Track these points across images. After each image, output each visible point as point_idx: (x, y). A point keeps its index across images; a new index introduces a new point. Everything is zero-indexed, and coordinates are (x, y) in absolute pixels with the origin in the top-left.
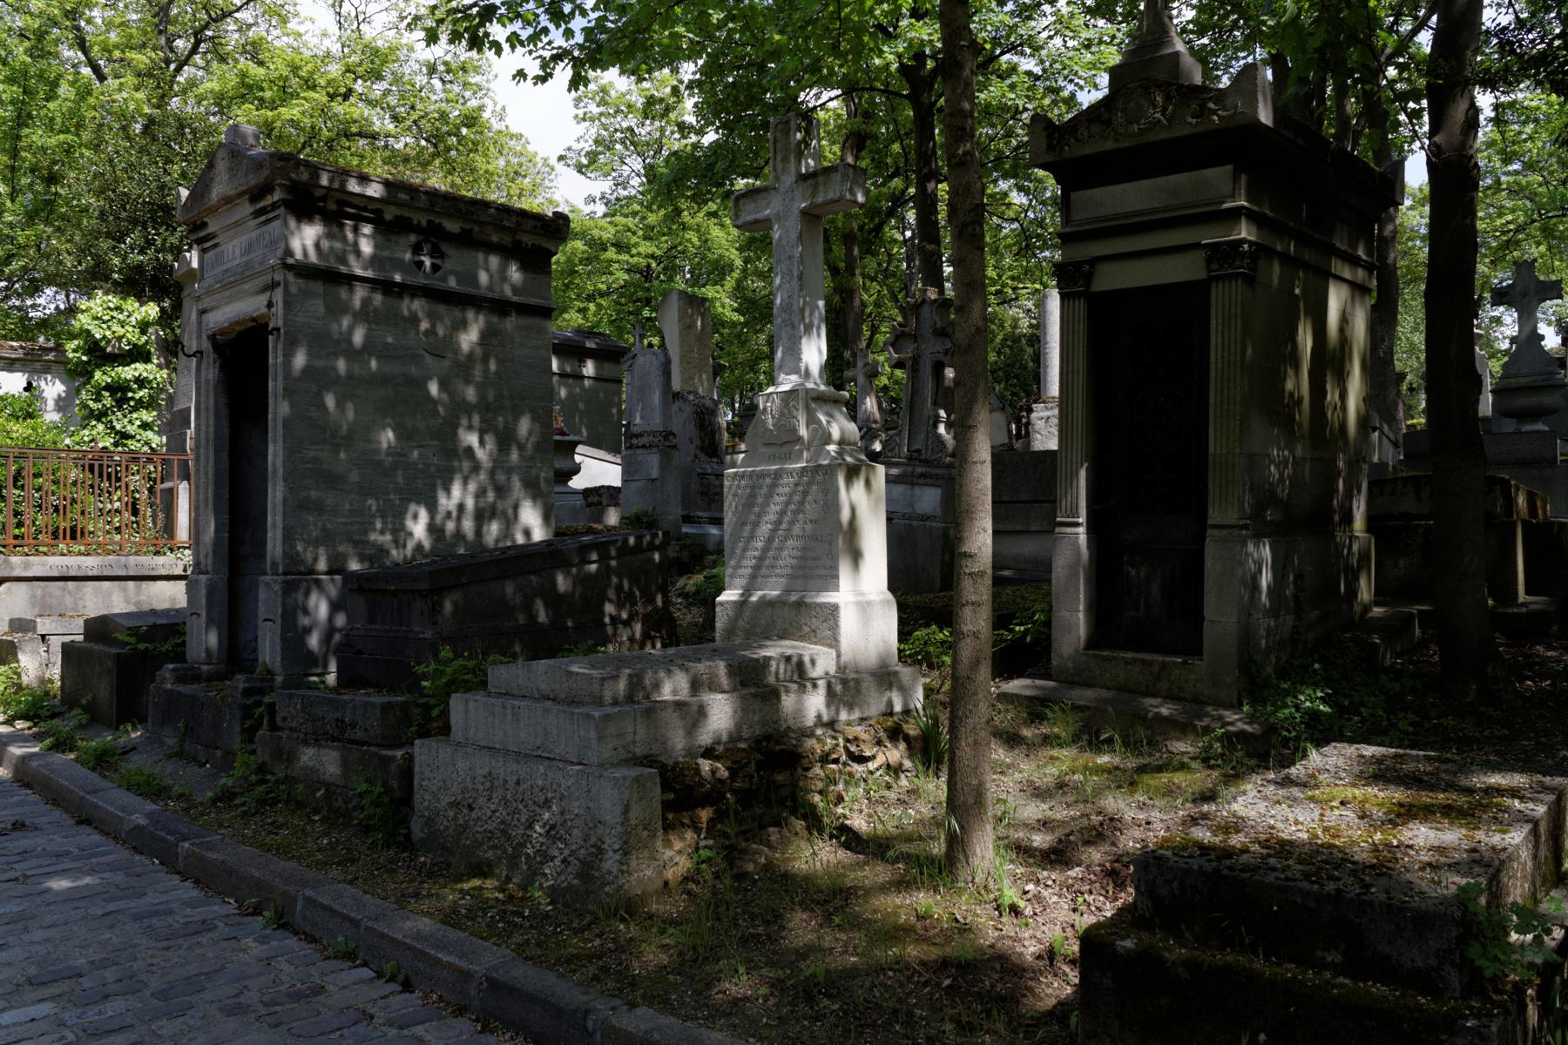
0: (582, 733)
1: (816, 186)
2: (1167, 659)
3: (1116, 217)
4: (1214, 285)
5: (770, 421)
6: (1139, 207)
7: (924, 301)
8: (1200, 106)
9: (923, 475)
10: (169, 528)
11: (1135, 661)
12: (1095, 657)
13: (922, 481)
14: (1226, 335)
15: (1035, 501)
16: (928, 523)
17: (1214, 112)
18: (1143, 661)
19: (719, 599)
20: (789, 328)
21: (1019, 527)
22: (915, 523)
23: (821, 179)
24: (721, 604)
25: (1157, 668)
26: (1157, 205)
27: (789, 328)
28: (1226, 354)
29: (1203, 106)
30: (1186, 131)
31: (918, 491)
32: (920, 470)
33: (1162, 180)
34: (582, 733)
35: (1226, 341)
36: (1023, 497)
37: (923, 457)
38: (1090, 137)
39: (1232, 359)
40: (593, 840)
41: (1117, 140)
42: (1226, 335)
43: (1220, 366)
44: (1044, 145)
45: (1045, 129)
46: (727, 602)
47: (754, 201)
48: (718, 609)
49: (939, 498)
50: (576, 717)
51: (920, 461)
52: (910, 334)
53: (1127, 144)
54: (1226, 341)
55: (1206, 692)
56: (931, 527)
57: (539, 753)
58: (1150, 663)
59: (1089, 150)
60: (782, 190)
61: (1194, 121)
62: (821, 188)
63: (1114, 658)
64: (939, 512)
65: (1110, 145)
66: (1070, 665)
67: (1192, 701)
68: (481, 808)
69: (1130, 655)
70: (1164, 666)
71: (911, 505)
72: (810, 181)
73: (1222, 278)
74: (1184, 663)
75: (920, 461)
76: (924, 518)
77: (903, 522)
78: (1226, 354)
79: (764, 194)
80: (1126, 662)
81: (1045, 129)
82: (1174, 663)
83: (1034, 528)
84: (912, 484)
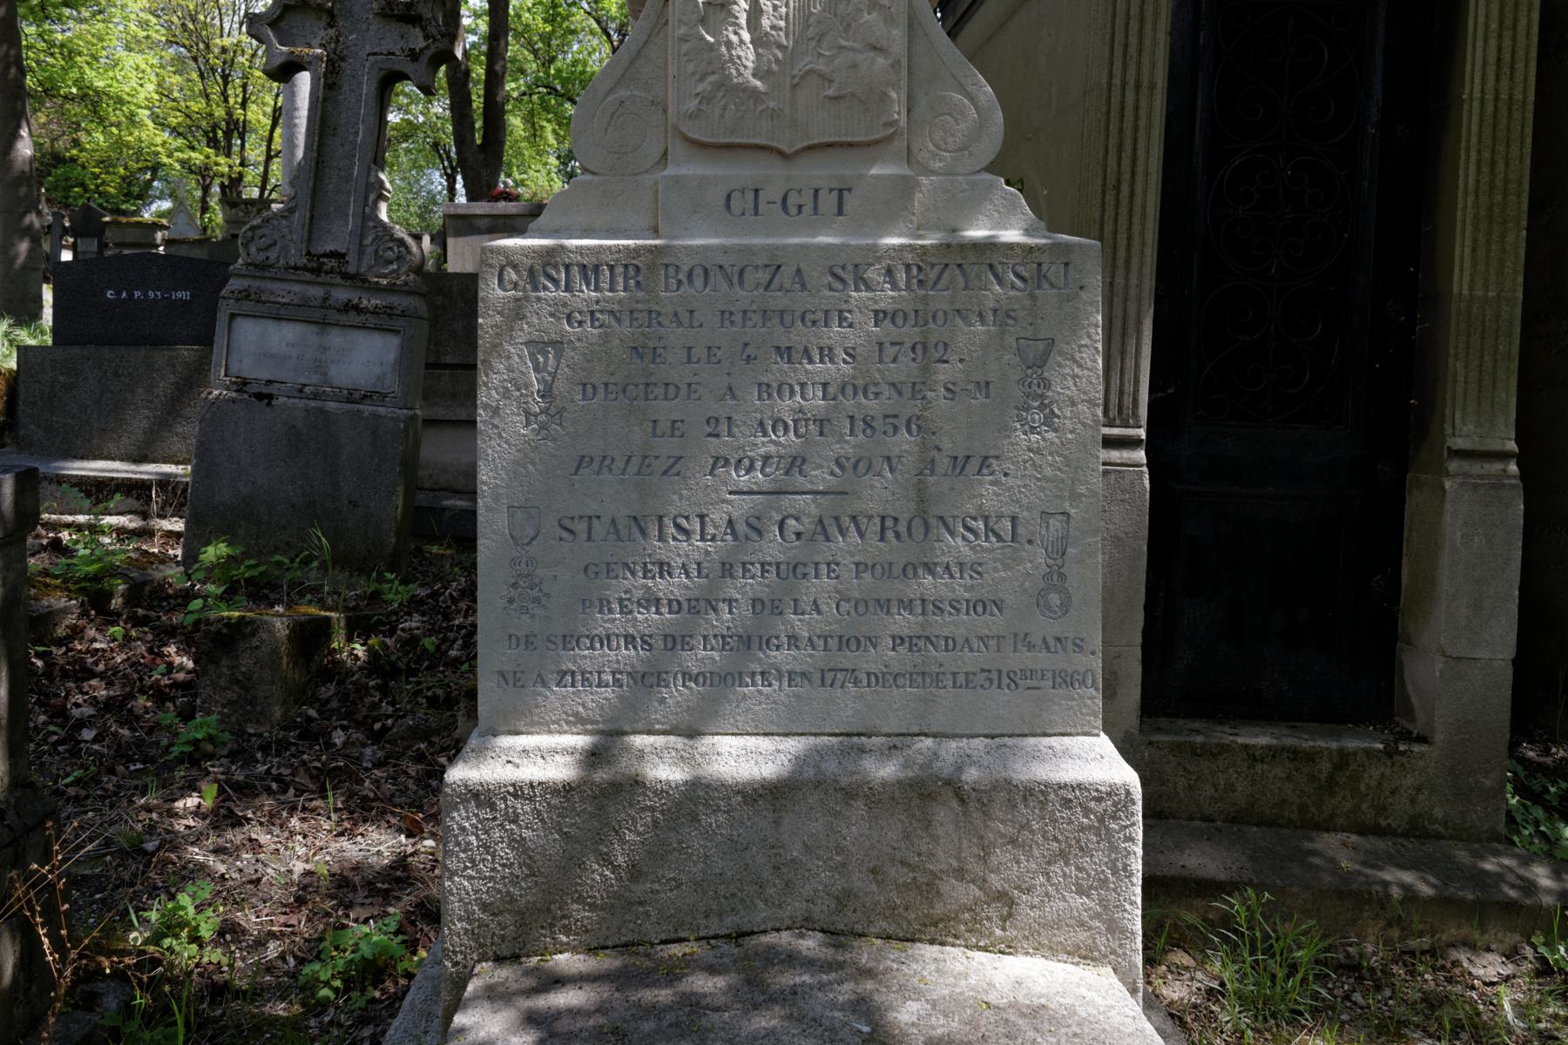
2: (1352, 744)
9: (349, 307)
11: (1273, 753)
13: (353, 317)
14: (1507, 42)
16: (367, 409)
18: (1295, 754)
22: (331, 406)
25: (1325, 766)
28: (1505, 83)
31: (336, 338)
32: (341, 295)
35: (1507, 56)
37: (351, 269)
39: (1518, 96)
42: (1507, 42)
43: (1490, 108)
51: (346, 276)
54: (1507, 56)
55: (1438, 813)
56: (377, 416)
58: (1311, 757)
63: (1224, 749)
64: (392, 384)
69: (1261, 739)
70: (1343, 760)
71: (320, 367)
75: (346, 276)
76: (352, 396)
77: (301, 403)
78: (1505, 83)
80: (1253, 756)
82: (1369, 753)
84: (323, 324)
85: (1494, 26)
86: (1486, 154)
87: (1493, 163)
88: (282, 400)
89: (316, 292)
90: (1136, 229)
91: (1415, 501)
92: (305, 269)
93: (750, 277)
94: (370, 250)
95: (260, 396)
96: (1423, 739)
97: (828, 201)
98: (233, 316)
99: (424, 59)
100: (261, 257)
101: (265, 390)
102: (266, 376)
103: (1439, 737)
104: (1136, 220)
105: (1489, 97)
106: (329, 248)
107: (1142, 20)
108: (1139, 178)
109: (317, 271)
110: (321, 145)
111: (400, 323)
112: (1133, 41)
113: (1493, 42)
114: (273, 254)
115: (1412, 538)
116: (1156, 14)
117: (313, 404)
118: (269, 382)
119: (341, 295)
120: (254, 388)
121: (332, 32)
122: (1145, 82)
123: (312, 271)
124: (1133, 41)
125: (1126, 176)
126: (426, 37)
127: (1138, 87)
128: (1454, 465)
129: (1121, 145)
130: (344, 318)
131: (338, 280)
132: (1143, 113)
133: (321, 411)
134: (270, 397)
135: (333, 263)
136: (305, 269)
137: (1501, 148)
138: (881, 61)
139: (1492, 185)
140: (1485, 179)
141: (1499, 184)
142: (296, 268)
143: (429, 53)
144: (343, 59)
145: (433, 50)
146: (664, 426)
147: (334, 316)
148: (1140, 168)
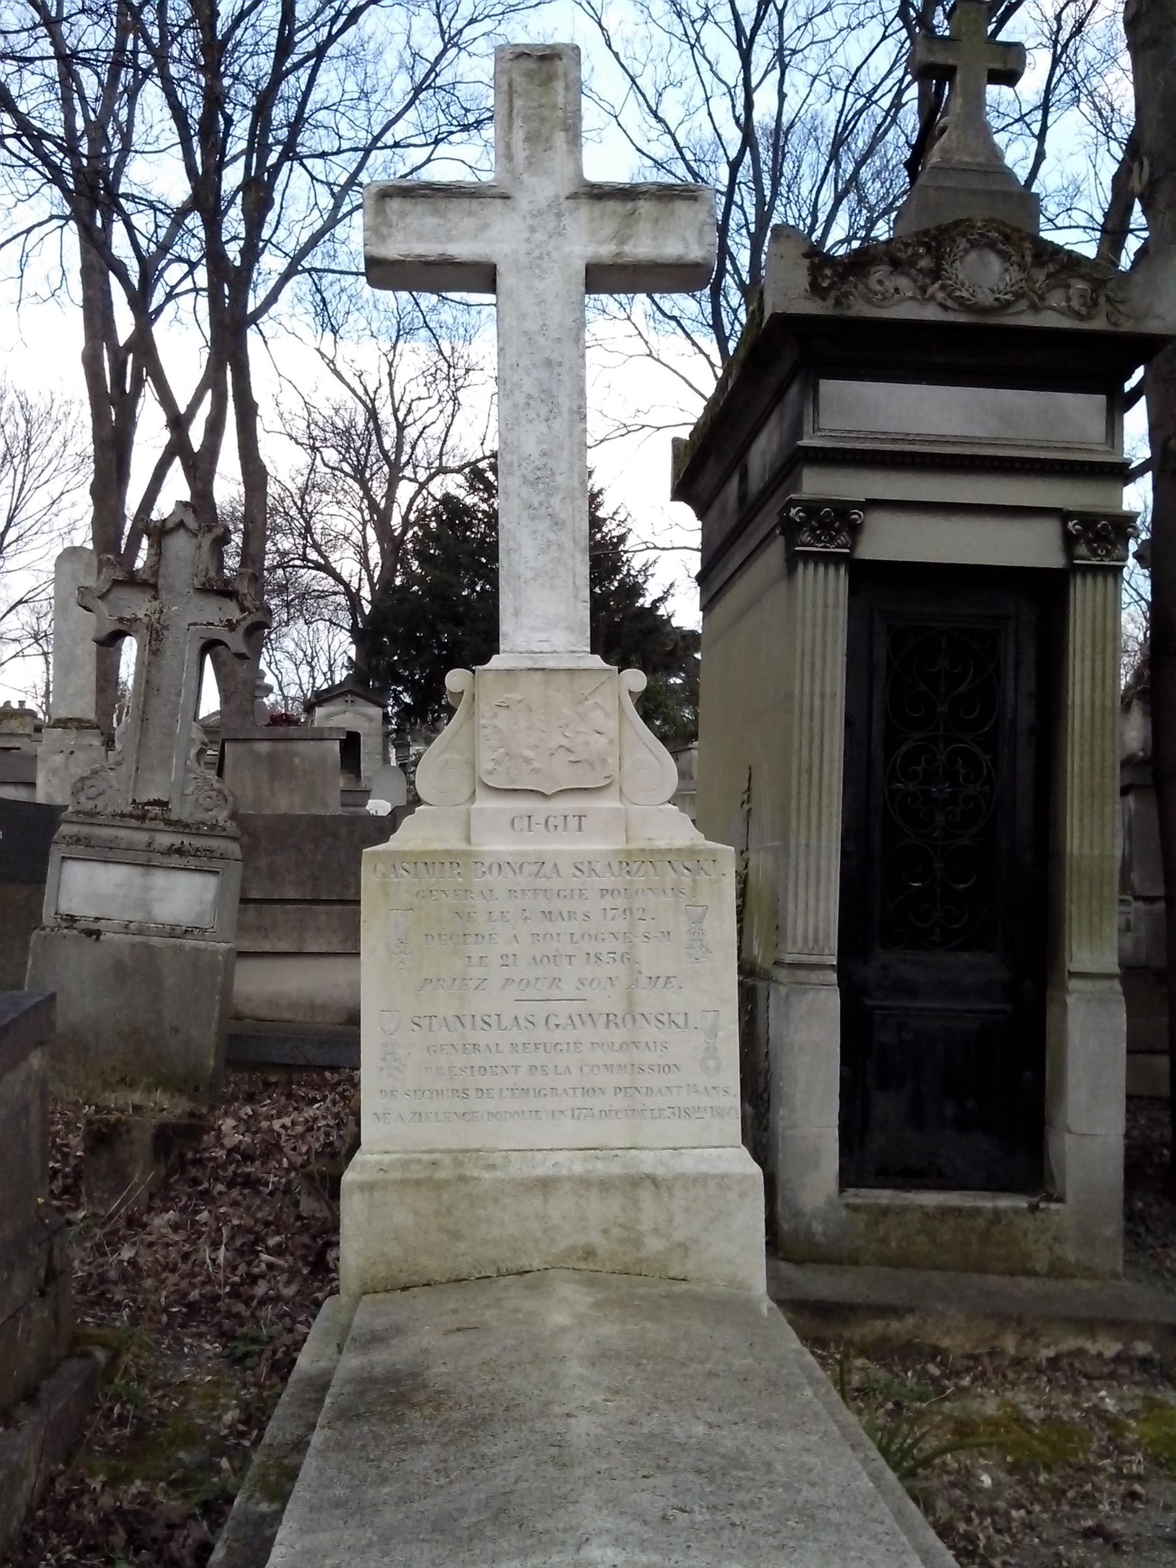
3: (873, 436)
4: (1079, 580)
9: (171, 851)
13: (175, 860)
14: (1099, 663)
16: (188, 943)
18: (958, 1212)
20: (543, 526)
21: (282, 946)
22: (156, 941)
26: (977, 432)
28: (1098, 691)
31: (160, 879)
32: (165, 840)
35: (1099, 674)
36: (291, 894)
37: (173, 816)
39: (1108, 703)
42: (1099, 663)
43: (1088, 713)
45: (806, 255)
47: (436, 212)
49: (210, 895)
51: (168, 822)
54: (1099, 674)
56: (197, 950)
62: (644, 227)
65: (931, 313)
66: (818, 1227)
71: (144, 905)
72: (611, 206)
75: (168, 822)
76: (174, 932)
78: (1098, 691)
79: (465, 203)
81: (806, 255)
82: (1016, 1211)
84: (148, 866)
85: (1088, 651)
86: (1087, 747)
87: (1092, 753)
88: (109, 935)
89: (142, 837)
90: (825, 802)
91: (1052, 1013)
92: (131, 816)
93: (526, 867)
94: (191, 799)
95: (89, 933)
96: (1060, 1200)
97: (573, 823)
98: (64, 858)
99: (241, 630)
100: (89, 805)
101: (95, 926)
102: (94, 914)
103: (1070, 1197)
104: (824, 796)
105: (1088, 704)
106: (154, 796)
107: (824, 645)
108: (826, 765)
109: (143, 818)
110: (145, 704)
111: (217, 865)
112: (818, 662)
113: (1088, 663)
114: (100, 802)
115: (1051, 1040)
116: (835, 640)
117: (138, 938)
118: (97, 919)
119: (165, 840)
120: (82, 925)
121: (156, 604)
122: (828, 691)
123: (137, 818)
124: (818, 662)
125: (816, 762)
126: (243, 609)
127: (823, 695)
128: (1073, 984)
129: (811, 740)
130: (167, 861)
131: (161, 826)
132: (827, 714)
133: (147, 946)
134: (98, 933)
135: (156, 810)
136: (131, 816)
137: (1098, 742)
139: (1092, 770)
140: (1087, 765)
141: (1097, 769)
142: (123, 815)
143: (244, 624)
144: (166, 628)
145: (248, 622)
146: (475, 960)
147: (157, 859)
148: (826, 758)
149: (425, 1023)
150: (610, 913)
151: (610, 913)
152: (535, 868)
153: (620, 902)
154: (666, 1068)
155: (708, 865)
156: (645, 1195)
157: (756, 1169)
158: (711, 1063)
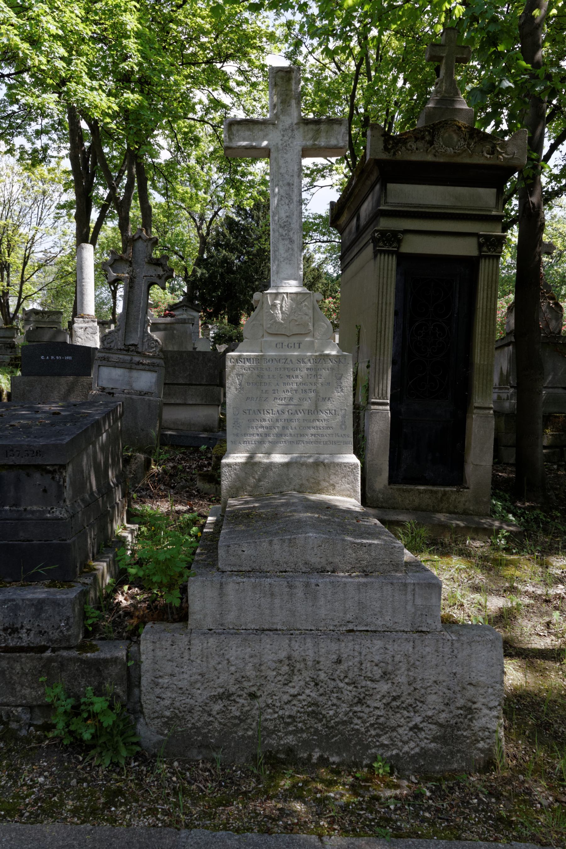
0: (419, 601)
1: (318, 131)
2: (447, 489)
4: (483, 261)
5: (280, 316)
6: (435, 203)
7: (140, 237)
8: (492, 148)
9: (139, 363)
10: (386, 396)
11: (426, 491)
12: (399, 490)
13: (141, 367)
14: (489, 292)
15: (192, 385)
16: (147, 398)
17: (501, 154)
18: (431, 491)
19: (224, 461)
20: (287, 242)
21: (178, 401)
22: (134, 397)
23: (323, 127)
24: (229, 465)
25: (440, 495)
26: (447, 203)
27: (287, 242)
28: (489, 304)
29: (494, 147)
30: (482, 161)
31: (135, 374)
32: (137, 359)
33: (451, 189)
34: (419, 601)
35: (489, 296)
38: (417, 149)
40: (461, 702)
41: (435, 156)
42: (489, 292)
43: (485, 311)
44: (382, 147)
45: (383, 136)
46: (236, 464)
47: (249, 130)
48: (224, 470)
49: (154, 380)
50: (410, 588)
51: (138, 352)
52: (127, 260)
53: (442, 160)
54: (489, 296)
56: (149, 400)
57: (350, 627)
58: (436, 492)
59: (414, 158)
60: (280, 127)
61: (488, 156)
62: (323, 134)
63: (412, 490)
64: (154, 389)
65: (430, 158)
66: (380, 496)
67: (462, 514)
68: (272, 695)
69: (422, 488)
70: (445, 493)
71: (130, 384)
72: (311, 126)
73: (486, 257)
74: (458, 491)
75: (138, 352)
76: (141, 393)
77: (124, 396)
78: (489, 304)
79: (260, 126)
80: (420, 492)
81: (383, 136)
82: (452, 491)
83: (191, 402)
84: (131, 369)
85: (486, 287)
86: (484, 324)
87: (486, 326)
88: (117, 395)
89: (128, 358)
90: (386, 344)
91: (468, 421)
92: (124, 350)
94: (146, 343)
95: (110, 393)
96: (468, 488)
98: (99, 366)
99: (163, 278)
100: (108, 346)
101: (111, 391)
102: (111, 386)
103: (471, 487)
104: (386, 341)
105: (485, 307)
106: (132, 342)
107: (387, 285)
108: (387, 330)
109: (128, 350)
110: (128, 307)
111: (157, 368)
112: (385, 291)
113: (485, 292)
114: (112, 345)
115: (467, 432)
116: (391, 284)
117: (128, 396)
118: (112, 389)
119: (137, 359)
120: (107, 391)
121: (131, 268)
122: (388, 302)
123: (126, 351)
124: (385, 291)
125: (383, 329)
126: (164, 271)
127: (386, 304)
128: (475, 411)
129: (381, 320)
130: (138, 367)
131: (135, 354)
132: (388, 311)
133: (131, 399)
134: (113, 394)
135: (133, 348)
136: (124, 350)
137: (488, 322)
138: (307, 317)
139: (485, 332)
140: (484, 330)
141: (488, 332)
142: (121, 350)
143: (165, 276)
144: (135, 278)
145: (166, 275)
146: (264, 391)
147: (134, 366)
148: (387, 326)
149: (247, 412)
150: (310, 376)
151: (310, 376)
152: (284, 361)
153: (313, 373)
154: (328, 428)
155: (343, 360)
156: (321, 469)
157: (358, 462)
158: (343, 427)
